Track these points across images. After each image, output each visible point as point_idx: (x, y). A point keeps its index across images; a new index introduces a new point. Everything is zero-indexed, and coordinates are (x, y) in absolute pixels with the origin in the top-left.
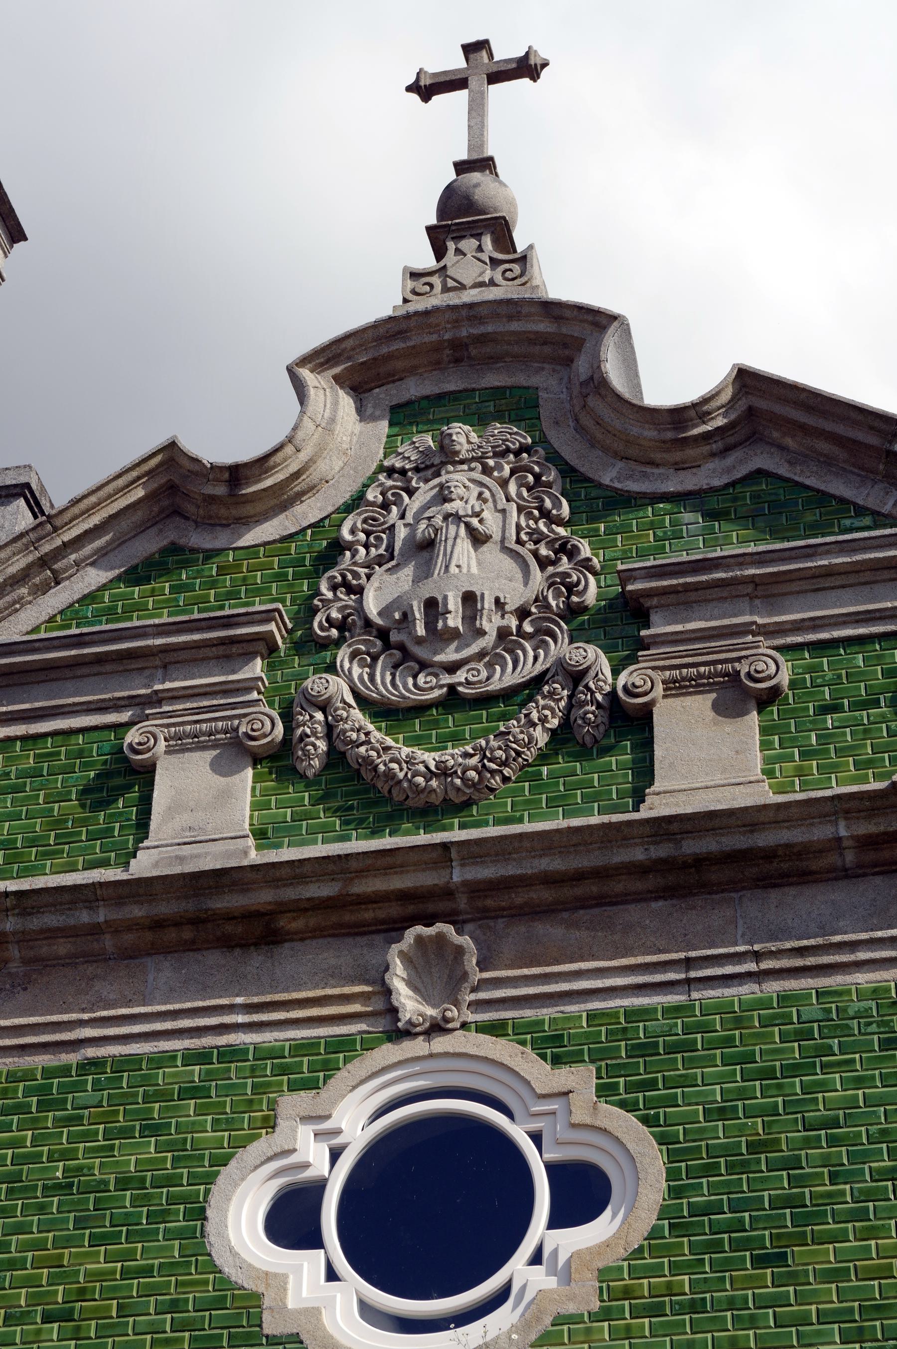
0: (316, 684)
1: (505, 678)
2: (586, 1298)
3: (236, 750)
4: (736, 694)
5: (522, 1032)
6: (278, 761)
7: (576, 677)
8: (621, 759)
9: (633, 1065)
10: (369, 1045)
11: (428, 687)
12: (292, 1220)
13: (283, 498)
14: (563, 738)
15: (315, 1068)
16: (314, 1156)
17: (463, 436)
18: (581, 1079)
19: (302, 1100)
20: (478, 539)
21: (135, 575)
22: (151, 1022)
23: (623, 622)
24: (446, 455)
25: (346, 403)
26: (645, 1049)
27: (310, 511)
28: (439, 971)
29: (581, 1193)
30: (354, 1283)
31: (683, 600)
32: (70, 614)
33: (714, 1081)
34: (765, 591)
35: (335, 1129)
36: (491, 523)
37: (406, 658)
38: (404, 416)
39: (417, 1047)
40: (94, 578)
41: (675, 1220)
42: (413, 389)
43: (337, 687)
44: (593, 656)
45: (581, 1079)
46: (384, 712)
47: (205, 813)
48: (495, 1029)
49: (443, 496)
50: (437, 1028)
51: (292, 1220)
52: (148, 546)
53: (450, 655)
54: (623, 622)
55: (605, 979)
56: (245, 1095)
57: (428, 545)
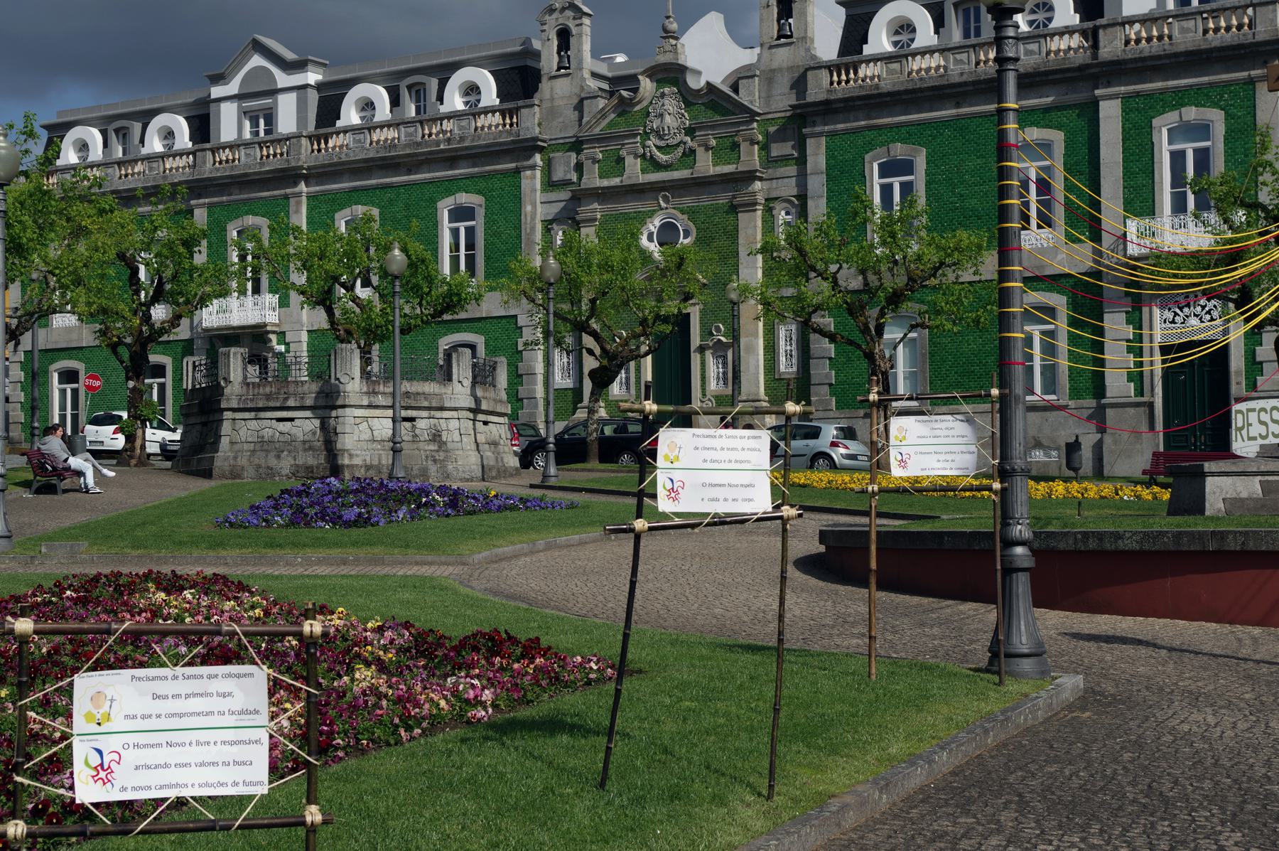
1: (675, 142)
3: (636, 156)
4: (707, 148)
6: (643, 156)
11: (662, 143)
13: (639, 102)
14: (684, 153)
15: (651, 214)
17: (667, 90)
21: (619, 115)
22: (630, 207)
23: (690, 131)
24: (663, 95)
25: (648, 80)
27: (645, 103)
28: (666, 200)
31: (701, 128)
32: (610, 125)
34: (713, 127)
37: (661, 137)
38: (658, 81)
40: (613, 116)
42: (660, 76)
43: (649, 143)
44: (688, 139)
45: (685, 217)
46: (657, 147)
47: (634, 171)
52: (620, 110)
54: (690, 131)
55: (688, 201)
56: (643, 218)
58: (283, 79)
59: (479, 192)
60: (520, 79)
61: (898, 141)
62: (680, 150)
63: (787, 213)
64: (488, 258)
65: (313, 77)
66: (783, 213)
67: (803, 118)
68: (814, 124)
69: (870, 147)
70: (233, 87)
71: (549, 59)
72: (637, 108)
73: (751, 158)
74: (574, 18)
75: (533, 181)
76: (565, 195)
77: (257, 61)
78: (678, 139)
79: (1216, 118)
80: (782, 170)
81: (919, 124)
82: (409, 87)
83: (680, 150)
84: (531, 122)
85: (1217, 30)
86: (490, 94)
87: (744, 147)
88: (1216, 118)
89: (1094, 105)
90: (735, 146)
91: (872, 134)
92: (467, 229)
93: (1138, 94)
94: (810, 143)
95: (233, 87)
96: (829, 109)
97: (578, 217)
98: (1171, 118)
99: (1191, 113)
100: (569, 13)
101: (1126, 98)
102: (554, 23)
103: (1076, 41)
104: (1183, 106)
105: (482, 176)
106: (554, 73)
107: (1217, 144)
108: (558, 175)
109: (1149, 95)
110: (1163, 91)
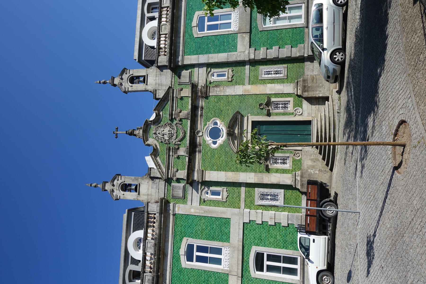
0: (174, 142)
2: (223, 123)
5: (204, 127)
7: (177, 124)
8: (183, 120)
9: (208, 119)
10: (203, 137)
11: (175, 134)
12: (215, 143)
13: (156, 146)
16: (210, 141)
18: (208, 123)
19: (207, 142)
20: (164, 131)
26: (206, 119)
29: (216, 123)
30: (220, 138)
33: (209, 114)
35: (209, 140)
36: (162, 130)
39: (204, 134)
41: (218, 117)
44: (175, 122)
45: (208, 123)
48: (203, 129)
49: (159, 133)
50: (203, 133)
51: (215, 143)
53: (173, 132)
57: (163, 134)
59: (181, 240)
61: (191, 24)
63: (213, 76)
64: (213, 239)
66: (213, 77)
67: (176, 68)
68: (179, 62)
69: (191, 35)
72: (158, 147)
73: (187, 92)
74: (118, 180)
75: (180, 209)
76: (189, 189)
80: (195, 77)
81: (186, 15)
87: (182, 95)
90: (182, 98)
91: (187, 35)
92: (197, 251)
94: (186, 62)
96: (173, 54)
97: (200, 181)
100: (115, 182)
102: (118, 191)
105: (174, 237)
106: (138, 193)
108: (180, 193)
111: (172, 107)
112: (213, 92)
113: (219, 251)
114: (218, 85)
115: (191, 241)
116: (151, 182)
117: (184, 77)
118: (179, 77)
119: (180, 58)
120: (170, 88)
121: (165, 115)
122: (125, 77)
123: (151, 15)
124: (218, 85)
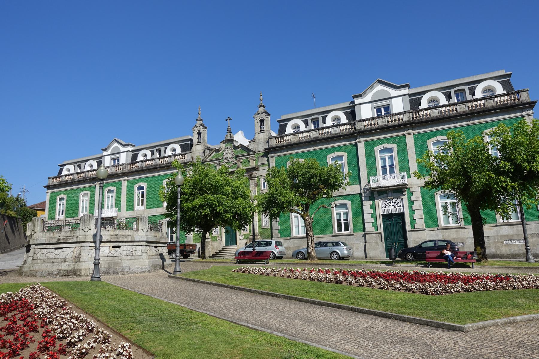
32: (212, 157)
58: (122, 149)
60: (187, 147)
62: (233, 163)
65: (130, 148)
70: (109, 152)
71: (195, 141)
73: (253, 164)
77: (116, 145)
78: (232, 160)
79: (394, 146)
82: (157, 150)
83: (233, 163)
84: (188, 157)
85: (392, 121)
86: (179, 151)
88: (394, 146)
89: (356, 145)
91: (288, 156)
93: (369, 141)
95: (109, 152)
98: (380, 147)
99: (386, 145)
100: (201, 127)
101: (365, 142)
103: (348, 127)
104: (384, 143)
107: (395, 154)
109: (372, 141)
110: (377, 140)
111: (244, 156)
112: (252, 183)
113: (142, 204)
114: (257, 185)
115: (145, 188)
116: (203, 151)
117: (263, 160)
118: (262, 156)
119: (273, 155)
120: (255, 152)
121: (240, 152)
122: (264, 116)
123: (310, 122)
124: (257, 185)
